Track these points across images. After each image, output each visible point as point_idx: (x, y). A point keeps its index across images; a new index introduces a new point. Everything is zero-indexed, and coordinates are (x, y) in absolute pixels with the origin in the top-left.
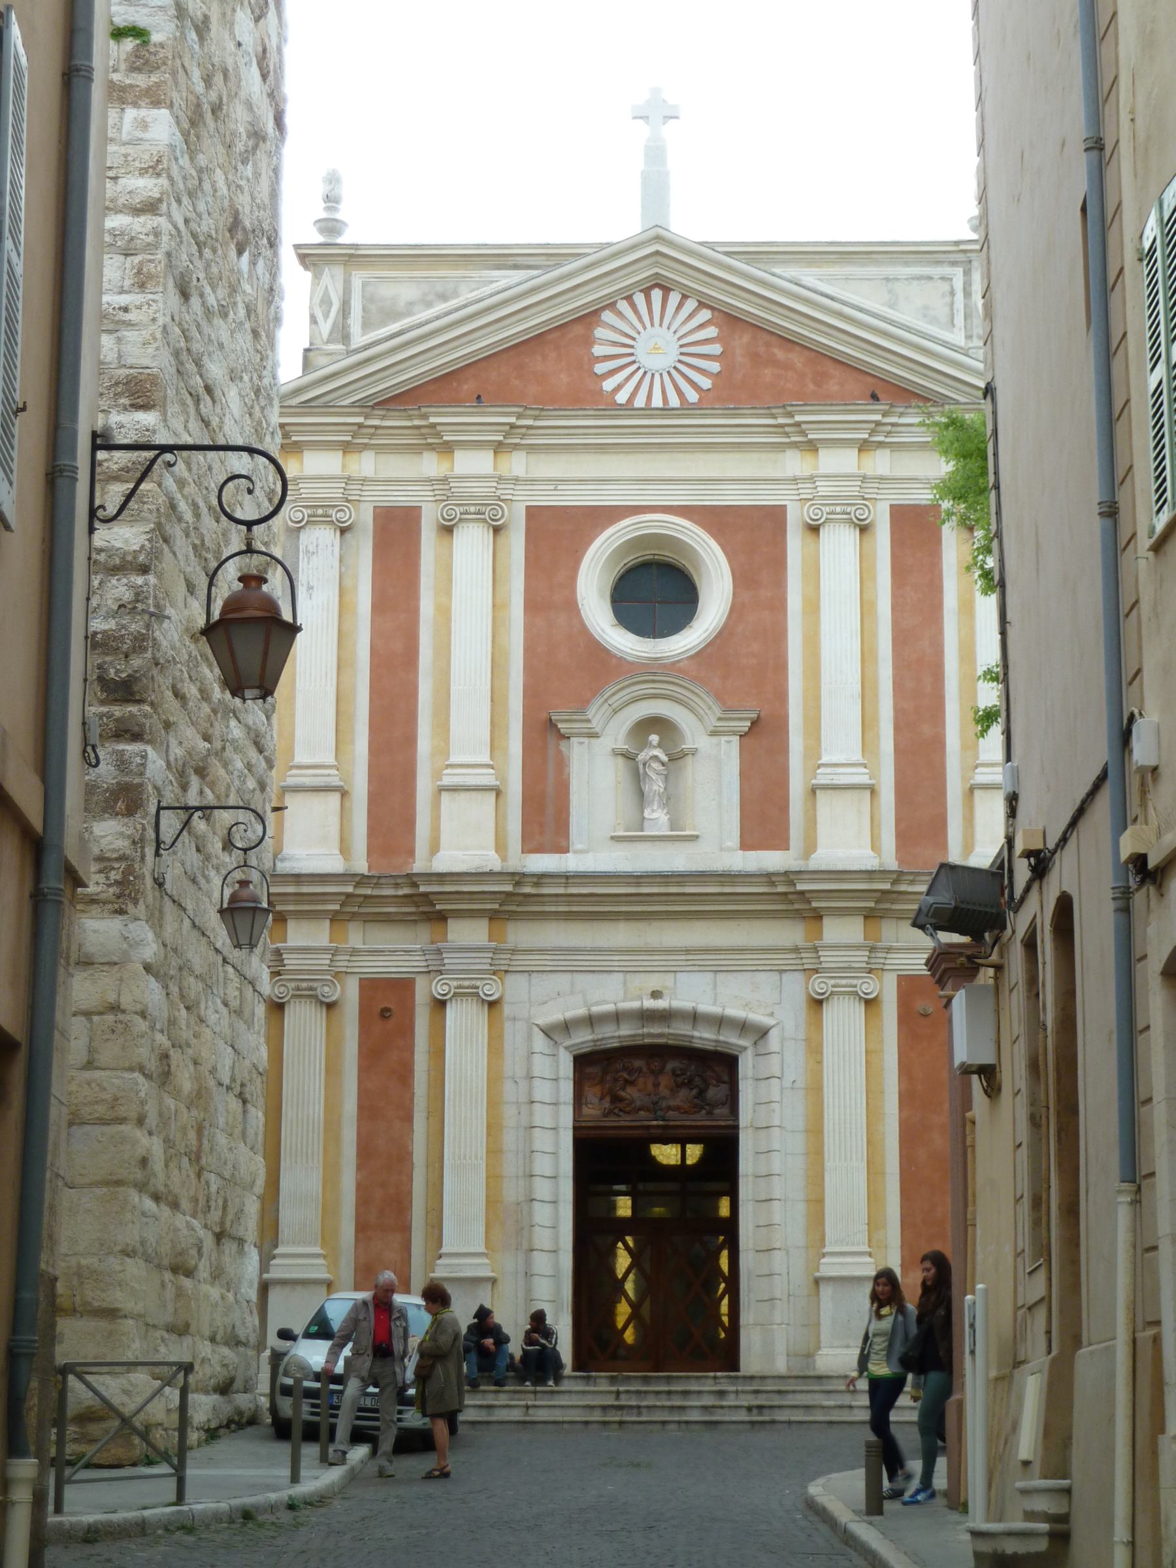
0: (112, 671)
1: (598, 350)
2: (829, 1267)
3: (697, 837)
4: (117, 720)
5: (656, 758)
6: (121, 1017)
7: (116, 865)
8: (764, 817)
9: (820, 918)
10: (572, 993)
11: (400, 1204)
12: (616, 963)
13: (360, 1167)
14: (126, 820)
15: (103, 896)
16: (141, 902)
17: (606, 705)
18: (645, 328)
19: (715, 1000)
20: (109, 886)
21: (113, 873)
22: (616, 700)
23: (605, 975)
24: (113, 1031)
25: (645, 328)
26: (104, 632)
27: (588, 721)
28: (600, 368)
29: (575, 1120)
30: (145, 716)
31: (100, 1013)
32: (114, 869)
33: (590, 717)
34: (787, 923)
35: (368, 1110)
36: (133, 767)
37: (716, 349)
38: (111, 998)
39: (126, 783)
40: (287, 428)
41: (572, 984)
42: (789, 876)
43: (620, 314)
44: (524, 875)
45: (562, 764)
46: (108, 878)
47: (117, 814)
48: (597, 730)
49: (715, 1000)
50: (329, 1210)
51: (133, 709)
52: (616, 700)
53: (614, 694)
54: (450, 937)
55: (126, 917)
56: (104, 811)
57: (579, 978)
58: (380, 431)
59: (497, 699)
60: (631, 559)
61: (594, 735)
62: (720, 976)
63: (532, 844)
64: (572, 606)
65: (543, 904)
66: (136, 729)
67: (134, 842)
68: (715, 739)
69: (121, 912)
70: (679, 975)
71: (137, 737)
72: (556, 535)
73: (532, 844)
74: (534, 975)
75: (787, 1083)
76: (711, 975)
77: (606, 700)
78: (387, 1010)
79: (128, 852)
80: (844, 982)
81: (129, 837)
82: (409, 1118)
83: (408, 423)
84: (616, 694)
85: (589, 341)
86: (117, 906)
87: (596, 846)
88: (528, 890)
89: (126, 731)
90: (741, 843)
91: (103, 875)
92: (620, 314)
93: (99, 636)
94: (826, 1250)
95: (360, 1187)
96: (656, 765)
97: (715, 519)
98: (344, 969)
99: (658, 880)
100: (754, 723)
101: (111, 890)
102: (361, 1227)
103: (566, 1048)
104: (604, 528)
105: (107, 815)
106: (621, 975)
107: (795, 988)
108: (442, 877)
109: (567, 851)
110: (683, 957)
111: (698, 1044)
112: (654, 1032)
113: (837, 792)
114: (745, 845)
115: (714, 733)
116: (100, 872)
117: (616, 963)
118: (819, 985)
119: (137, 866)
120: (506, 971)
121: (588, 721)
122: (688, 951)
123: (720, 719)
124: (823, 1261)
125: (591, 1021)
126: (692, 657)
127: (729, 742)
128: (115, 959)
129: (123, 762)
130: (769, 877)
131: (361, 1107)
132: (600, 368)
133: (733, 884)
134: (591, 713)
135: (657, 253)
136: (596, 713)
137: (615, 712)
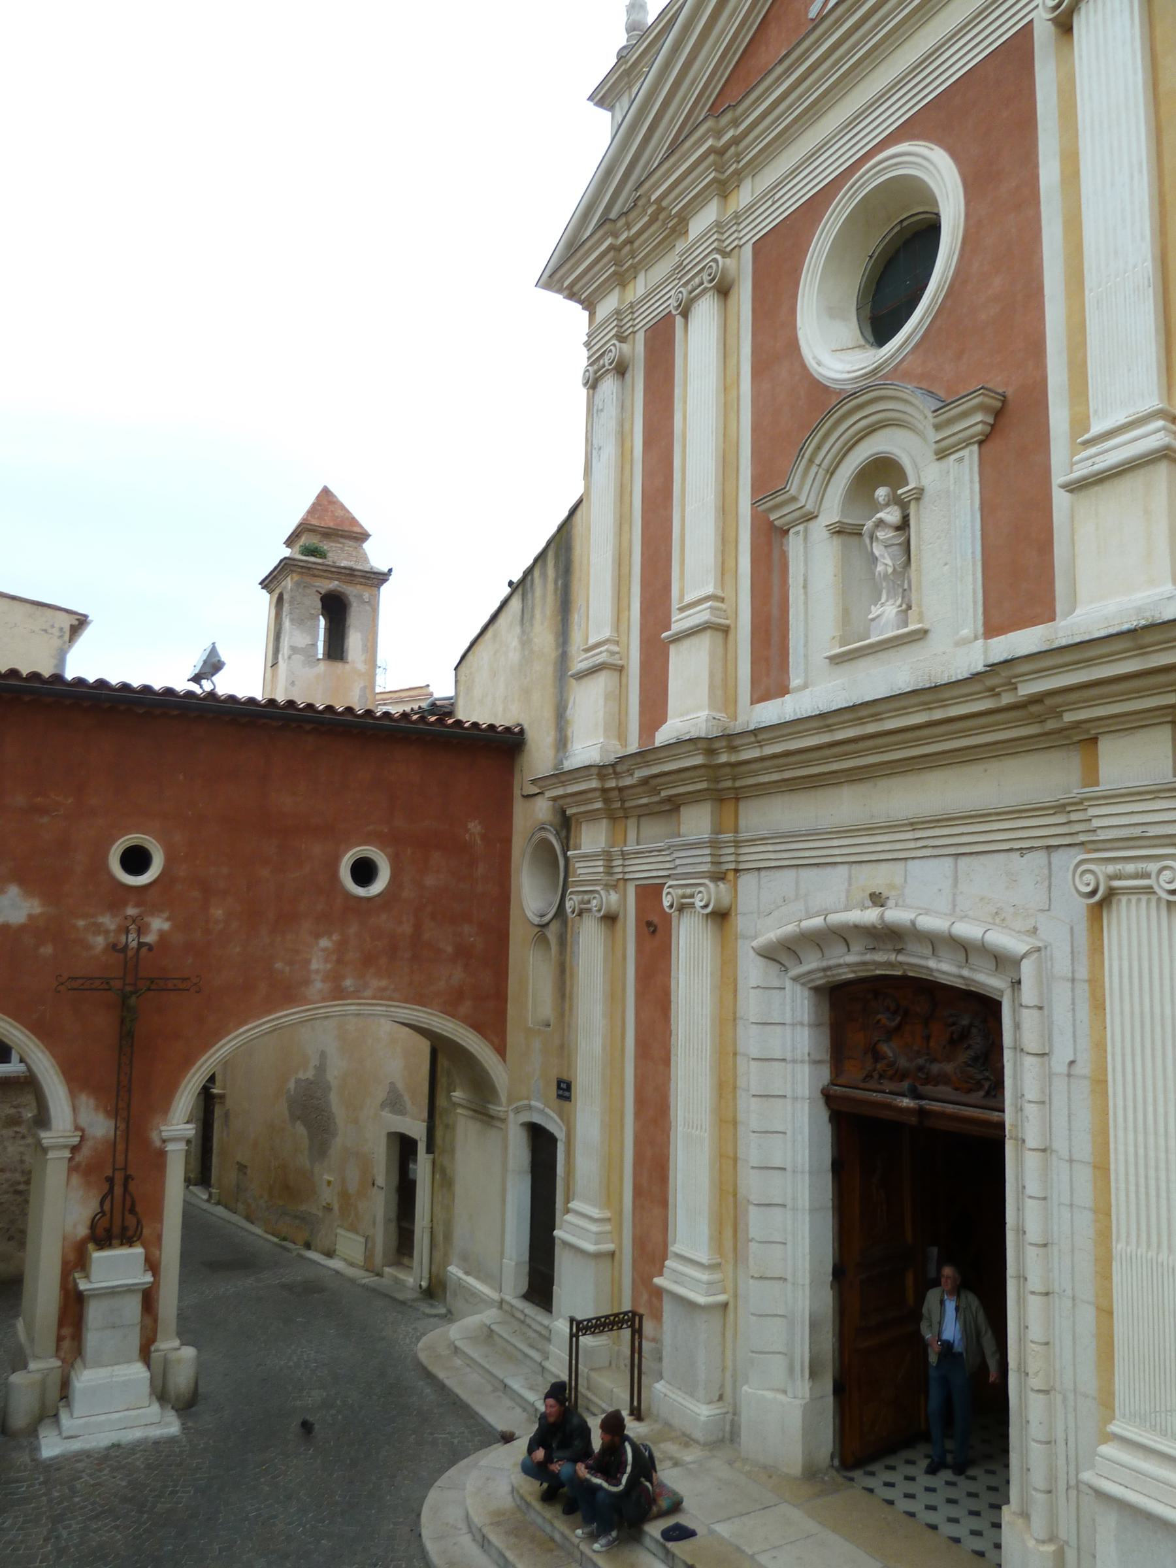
3: (926, 632)
8: (1020, 572)
9: (1094, 740)
12: (837, 851)
17: (814, 469)
22: (825, 456)
23: (829, 870)
27: (794, 499)
33: (793, 492)
34: (1056, 756)
40: (575, 289)
41: (797, 883)
48: (809, 507)
52: (825, 456)
53: (819, 448)
54: (684, 829)
57: (804, 873)
58: (636, 244)
60: (875, 242)
61: (810, 517)
62: (963, 862)
65: (755, 774)
70: (910, 863)
74: (763, 873)
75: (1059, 1064)
76: (950, 860)
77: (811, 461)
80: (1130, 868)
83: (646, 218)
88: (724, 758)
90: (986, 624)
94: (1114, 1428)
98: (620, 876)
99: (846, 717)
100: (998, 414)
103: (795, 979)
107: (1073, 875)
110: (909, 835)
112: (882, 959)
113: (1107, 486)
117: (837, 851)
120: (736, 871)
121: (794, 499)
122: (913, 825)
126: (917, 346)
127: (961, 460)
133: (943, 704)
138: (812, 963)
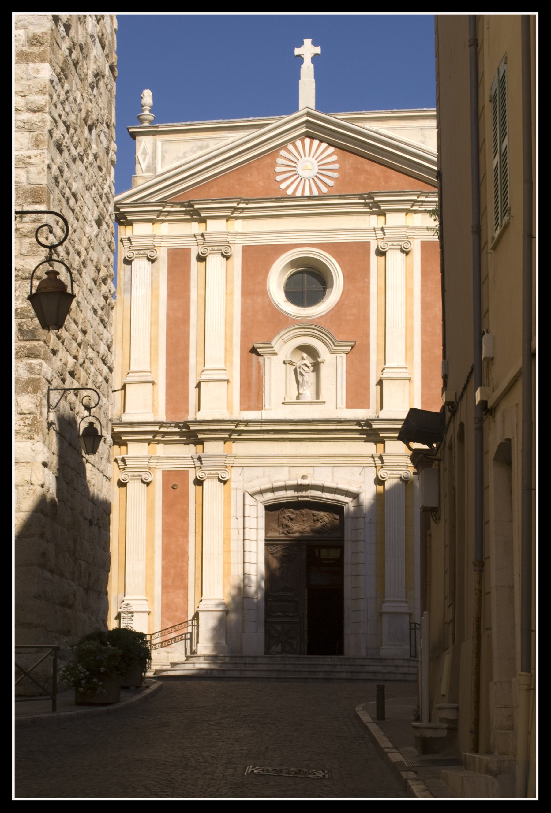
0: (25, 326)
1: (278, 169)
2: (387, 607)
3: (324, 402)
4: (28, 349)
5: (305, 365)
6: (31, 487)
7: (28, 416)
10: (264, 476)
11: (182, 576)
13: (164, 558)
14: (32, 395)
15: (22, 431)
16: (40, 433)
17: (281, 340)
18: (301, 157)
19: (333, 480)
20: (25, 426)
21: (27, 420)
22: (286, 337)
24: (28, 494)
25: (301, 157)
26: (21, 308)
27: (272, 347)
28: (279, 178)
29: (266, 537)
30: (41, 347)
31: (22, 486)
32: (27, 418)
35: (167, 532)
36: (36, 371)
37: (336, 166)
38: (28, 478)
39: (33, 378)
42: (368, 422)
43: (289, 152)
44: (240, 421)
45: (260, 368)
46: (25, 423)
47: (28, 393)
48: (276, 351)
49: (333, 480)
50: (149, 579)
51: (35, 343)
55: (33, 441)
56: (22, 392)
59: (228, 338)
61: (276, 354)
62: (336, 468)
63: (245, 406)
64: (264, 293)
66: (37, 353)
67: (37, 406)
68: (334, 356)
69: (31, 438)
71: (37, 357)
72: (257, 259)
73: (245, 406)
77: (281, 337)
78: (176, 485)
79: (34, 410)
81: (34, 403)
82: (186, 536)
84: (286, 334)
85: (273, 165)
86: (29, 436)
87: (276, 406)
89: (32, 354)
91: (22, 421)
92: (289, 152)
93: (19, 310)
95: (163, 568)
96: (305, 368)
97: (333, 248)
101: (26, 428)
102: (165, 587)
103: (261, 502)
104: (280, 255)
105: (24, 394)
106: (287, 468)
108: (200, 422)
109: (261, 409)
111: (325, 501)
114: (348, 407)
115: (332, 353)
116: (21, 420)
118: (381, 473)
119: (38, 417)
120: (232, 467)
121: (272, 347)
122: (320, 457)
123: (335, 346)
124: (383, 605)
125: (273, 490)
127: (340, 357)
128: (29, 460)
129: (31, 368)
130: (358, 422)
131: (163, 531)
132: (279, 178)
134: (273, 344)
135: (307, 121)
136: (276, 343)
137: (285, 342)
138: (269, 496)
